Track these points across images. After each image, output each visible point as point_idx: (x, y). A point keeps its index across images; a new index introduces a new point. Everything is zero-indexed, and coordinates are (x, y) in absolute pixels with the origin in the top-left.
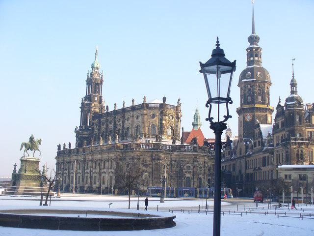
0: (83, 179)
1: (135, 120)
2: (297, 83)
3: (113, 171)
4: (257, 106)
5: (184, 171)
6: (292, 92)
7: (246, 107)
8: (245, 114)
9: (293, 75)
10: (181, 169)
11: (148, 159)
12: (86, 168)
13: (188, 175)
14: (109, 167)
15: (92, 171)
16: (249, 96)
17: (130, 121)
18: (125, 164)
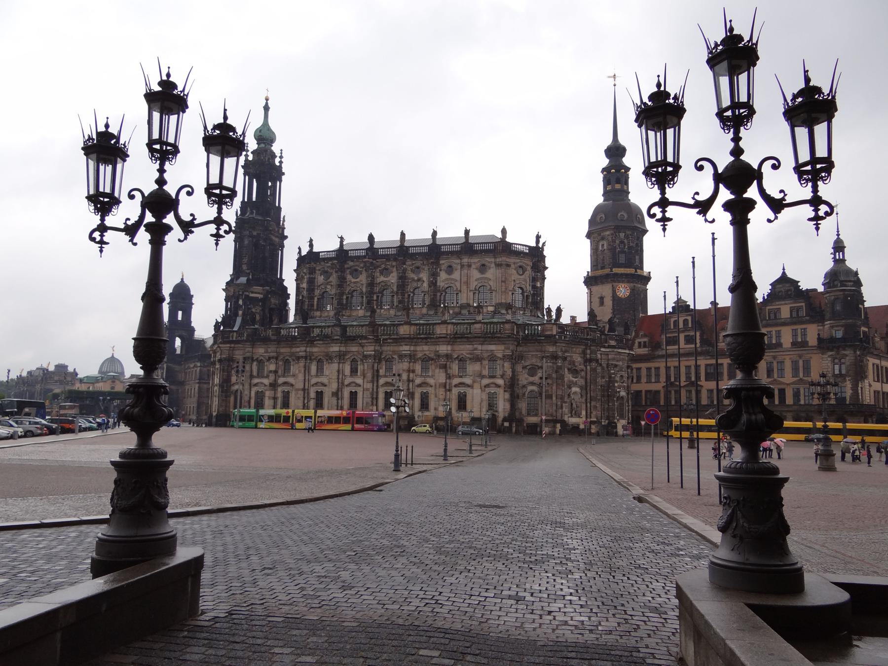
0: (374, 399)
1: (475, 274)
2: (845, 245)
3: (500, 382)
4: (639, 272)
5: (616, 385)
6: (836, 261)
7: (616, 270)
8: (615, 284)
9: (838, 232)
10: (611, 381)
11: (578, 359)
12: (382, 372)
13: (623, 393)
14: (485, 372)
15: (413, 381)
16: (622, 252)
17: (456, 275)
18: (524, 368)
